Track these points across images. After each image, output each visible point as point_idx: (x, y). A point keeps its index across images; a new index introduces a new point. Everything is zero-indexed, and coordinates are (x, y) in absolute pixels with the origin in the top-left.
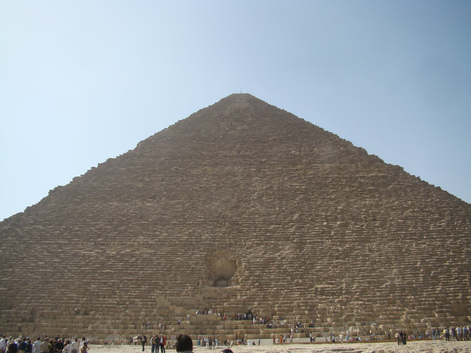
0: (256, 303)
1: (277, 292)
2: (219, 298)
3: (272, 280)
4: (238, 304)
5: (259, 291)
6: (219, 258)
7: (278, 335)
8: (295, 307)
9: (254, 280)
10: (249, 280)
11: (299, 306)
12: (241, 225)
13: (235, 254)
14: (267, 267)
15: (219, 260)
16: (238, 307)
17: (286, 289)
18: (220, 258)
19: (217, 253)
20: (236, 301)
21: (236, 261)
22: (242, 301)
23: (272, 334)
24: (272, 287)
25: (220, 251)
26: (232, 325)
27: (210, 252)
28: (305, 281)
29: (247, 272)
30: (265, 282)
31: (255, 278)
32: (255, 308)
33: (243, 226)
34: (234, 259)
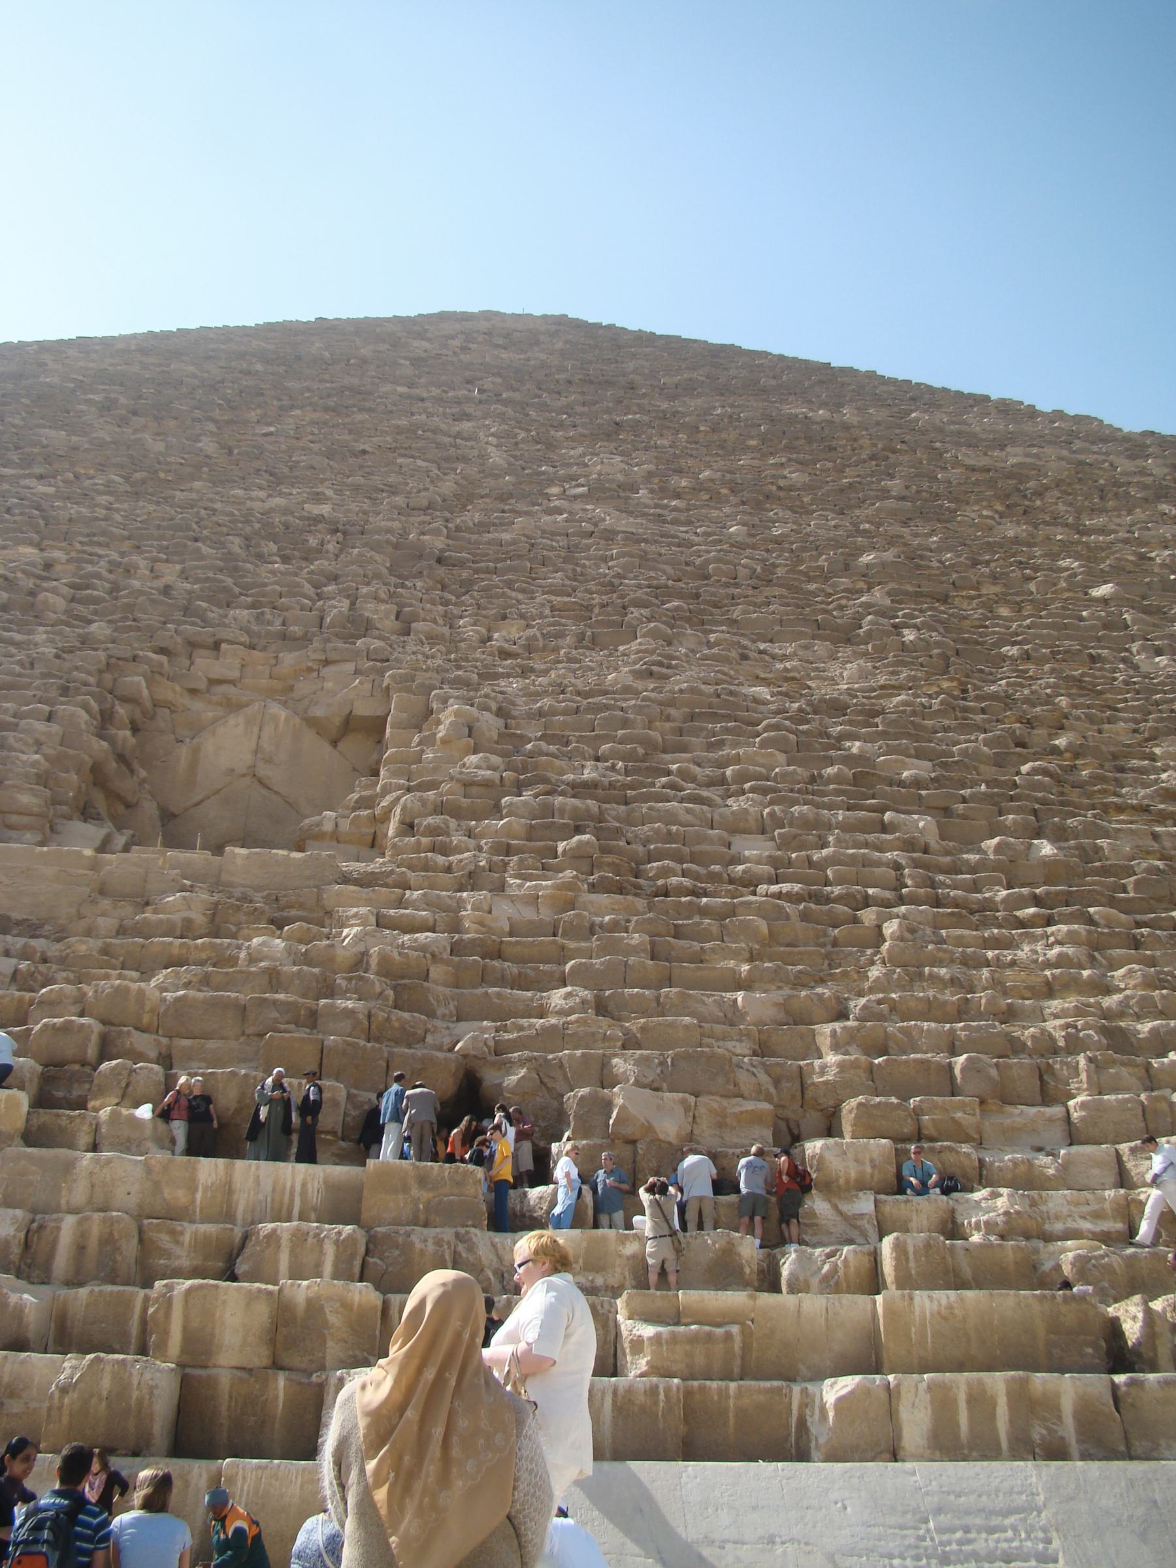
0: (557, 997)
1: (805, 916)
2: (106, 924)
3: (737, 827)
4: (330, 991)
5: (603, 899)
6: (232, 707)
7: (943, 1405)
8: (1074, 1045)
9: (548, 811)
10: (496, 811)
11: (1118, 1041)
12: (461, 564)
13: (381, 672)
14: (684, 749)
15: (235, 726)
16: (312, 1019)
17: (902, 900)
18: (240, 706)
19: (227, 665)
20: (307, 959)
21: (375, 728)
22: (387, 969)
23: (835, 1390)
24: (750, 883)
25: (256, 654)
26: (174, 1215)
27: (162, 651)
28: (1089, 855)
29: (473, 759)
30: (670, 837)
31: (558, 800)
32: (556, 1037)
33: (477, 571)
34: (364, 709)
